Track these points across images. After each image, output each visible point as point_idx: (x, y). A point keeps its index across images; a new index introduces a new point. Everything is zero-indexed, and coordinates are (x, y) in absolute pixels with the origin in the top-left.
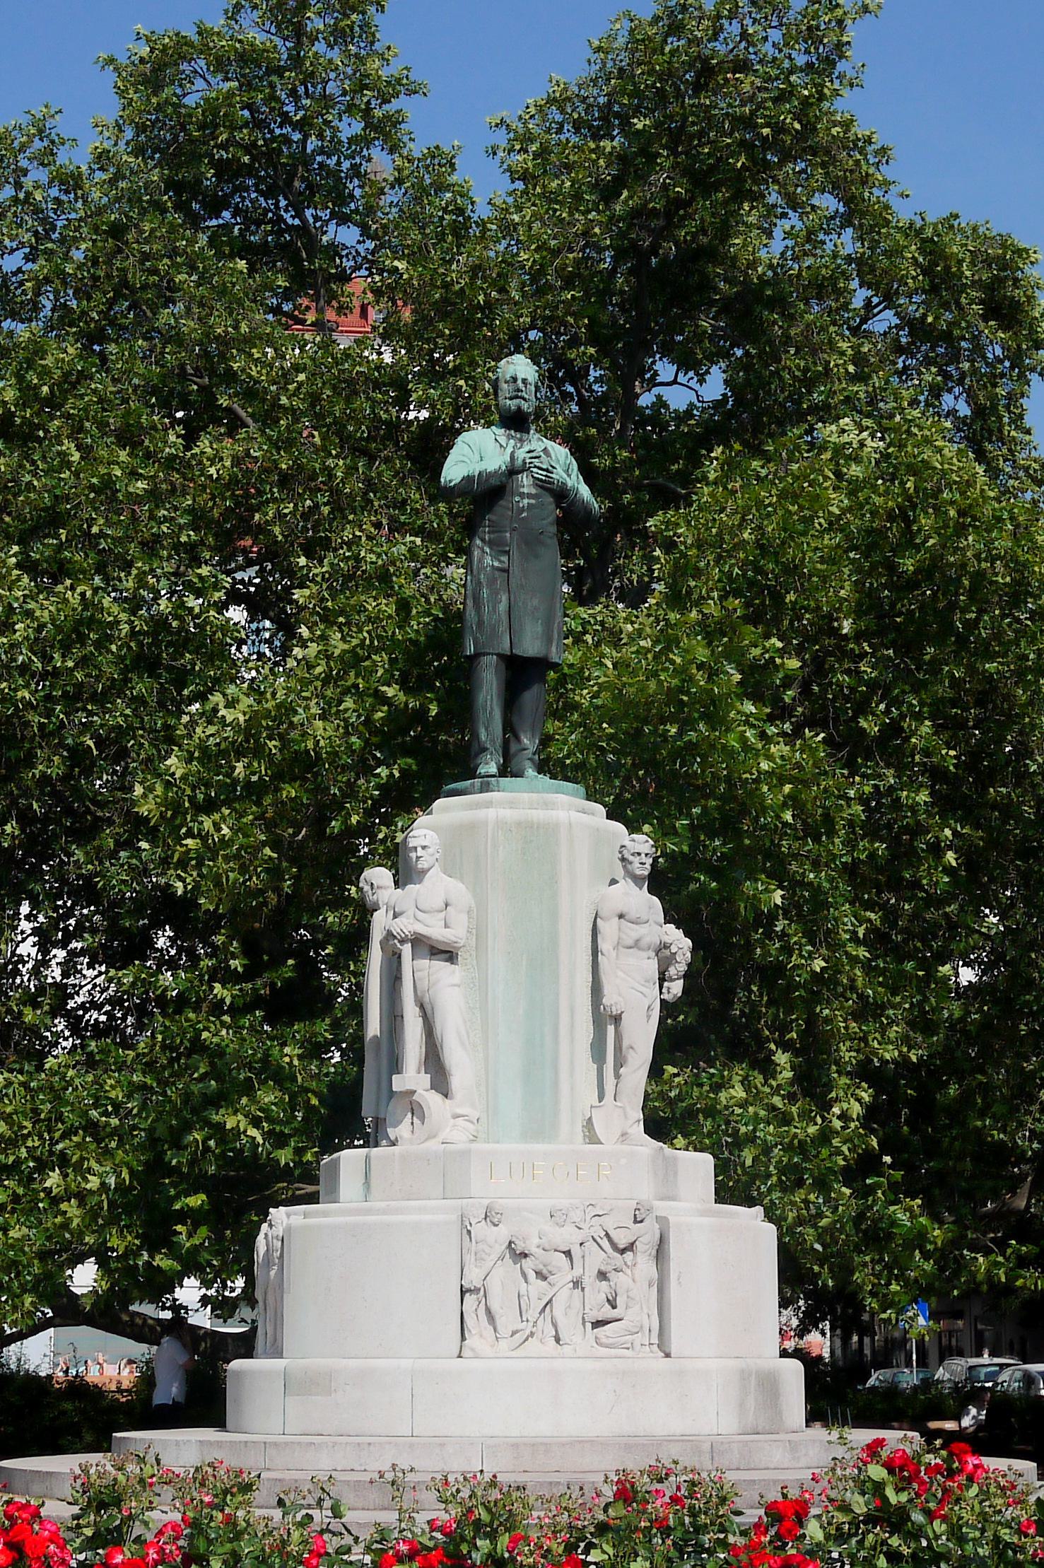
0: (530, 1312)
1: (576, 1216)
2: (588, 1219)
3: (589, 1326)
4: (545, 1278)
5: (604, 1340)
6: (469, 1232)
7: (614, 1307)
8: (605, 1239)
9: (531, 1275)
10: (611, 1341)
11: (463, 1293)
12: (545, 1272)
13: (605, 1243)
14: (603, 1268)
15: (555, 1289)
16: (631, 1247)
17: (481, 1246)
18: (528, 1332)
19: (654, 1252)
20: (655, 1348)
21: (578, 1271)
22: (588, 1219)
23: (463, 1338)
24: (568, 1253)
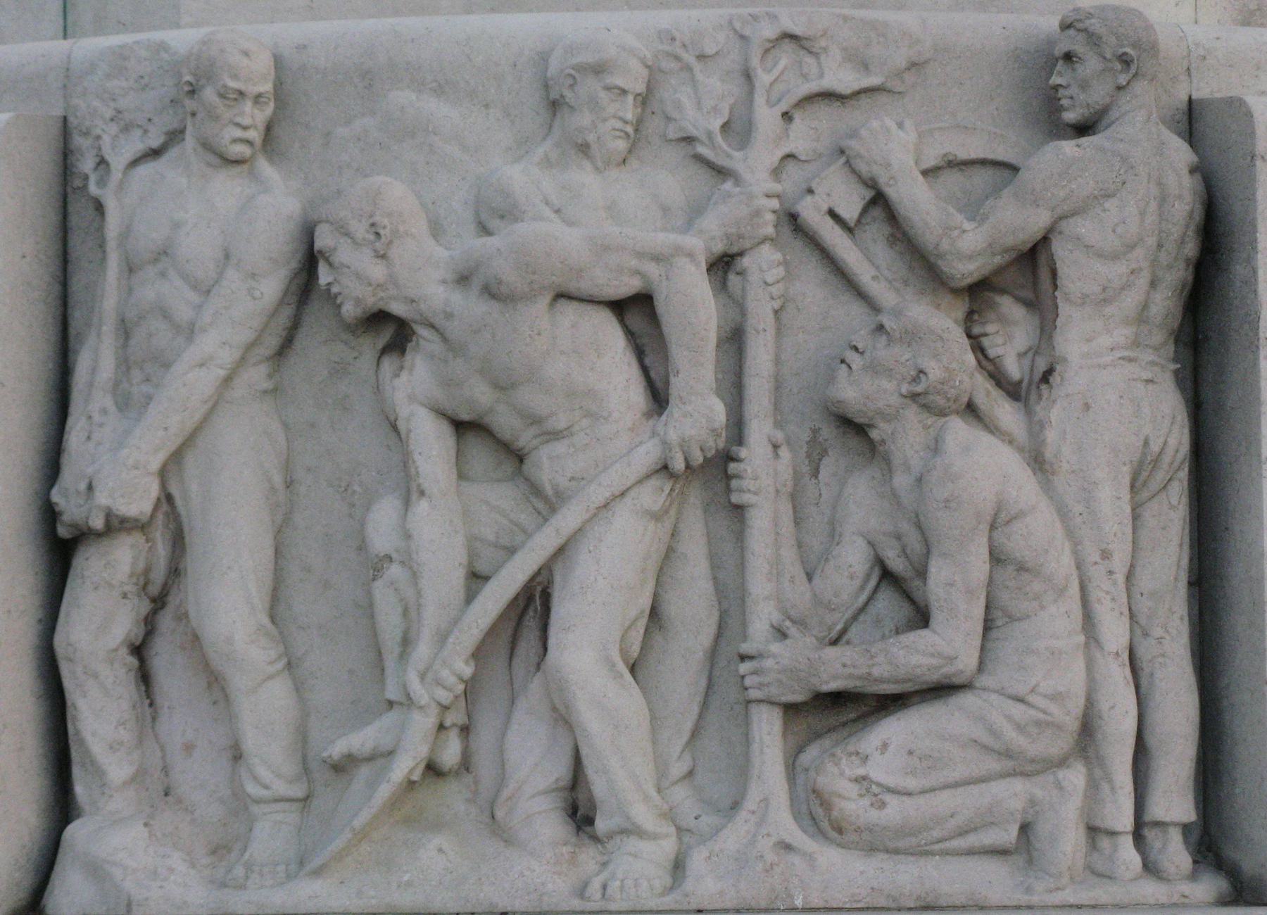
0: (423, 650)
1: (700, 106)
2: (766, 117)
3: (768, 729)
4: (515, 456)
5: (853, 806)
6: (99, 207)
7: (921, 617)
8: (876, 232)
9: (431, 445)
10: (895, 811)
11: (60, 549)
12: (505, 422)
13: (867, 259)
14: (851, 392)
15: (568, 519)
16: (1030, 269)
17: (149, 290)
18: (405, 765)
19: (1165, 303)
20: (1176, 854)
21: (698, 413)
23: (62, 806)
24: (636, 311)
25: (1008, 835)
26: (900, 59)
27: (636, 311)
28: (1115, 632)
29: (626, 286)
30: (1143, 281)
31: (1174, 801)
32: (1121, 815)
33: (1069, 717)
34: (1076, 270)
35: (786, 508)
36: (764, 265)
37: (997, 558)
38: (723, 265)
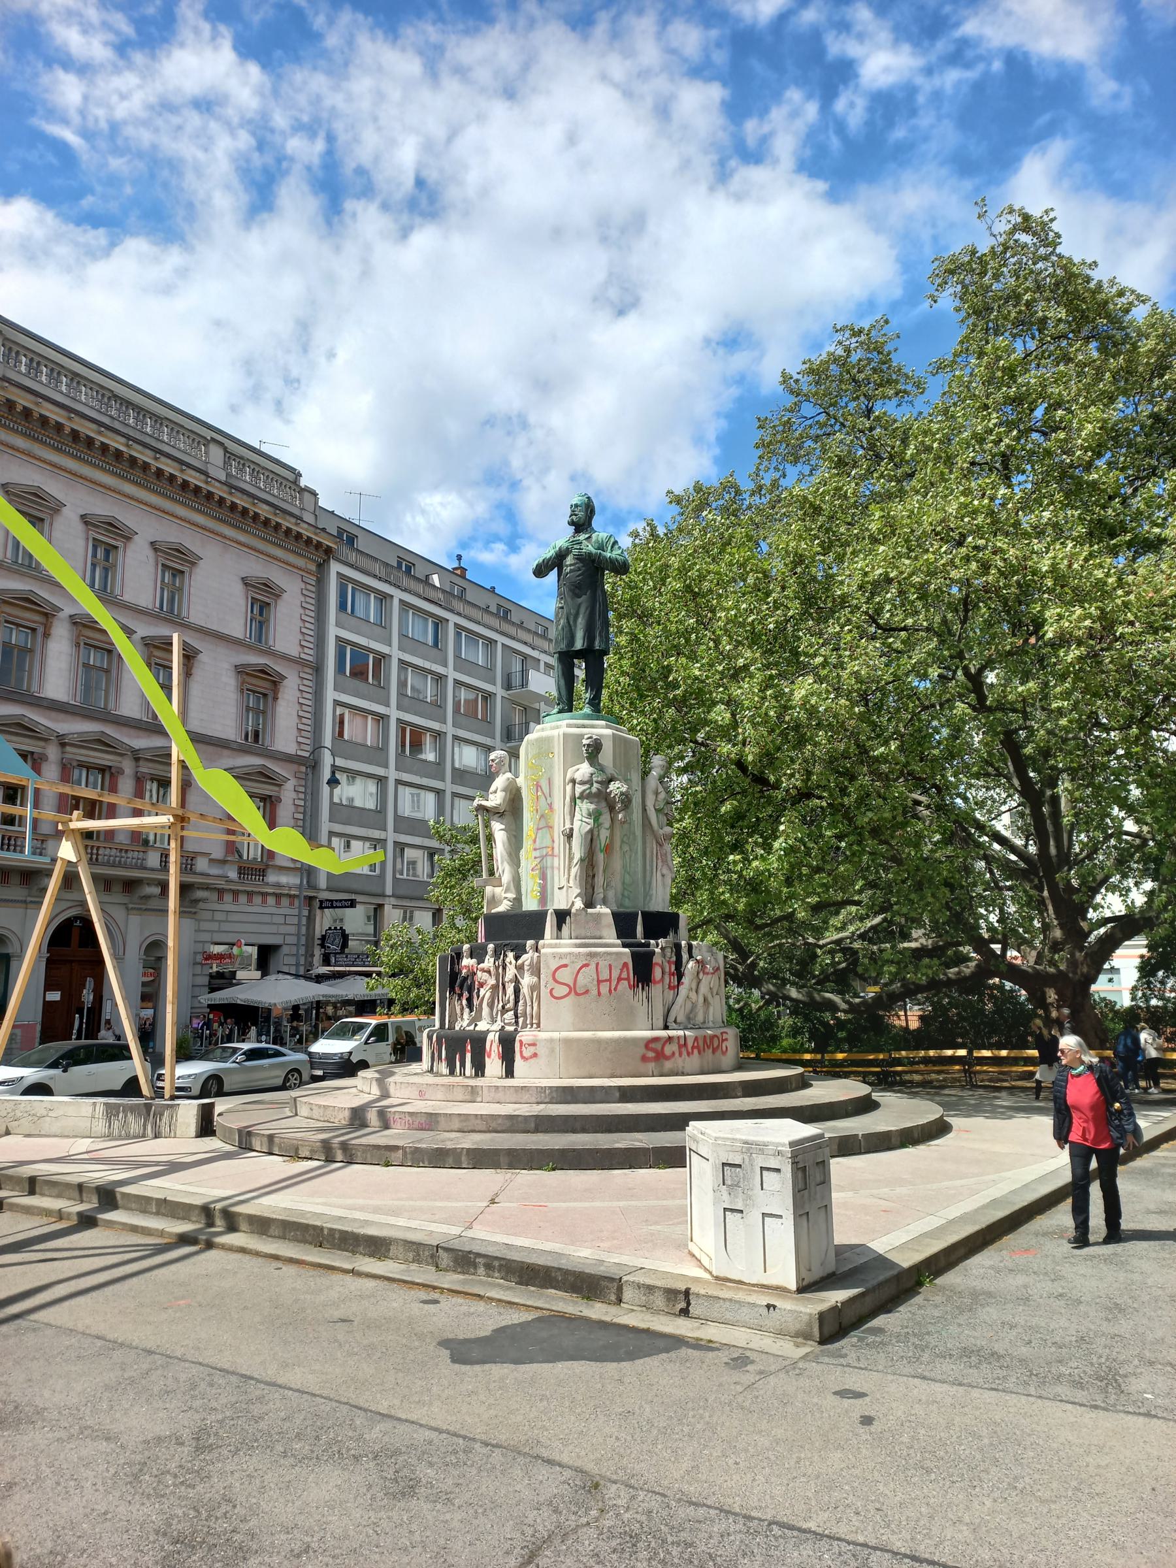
28: (529, 1003)
34: (526, 968)
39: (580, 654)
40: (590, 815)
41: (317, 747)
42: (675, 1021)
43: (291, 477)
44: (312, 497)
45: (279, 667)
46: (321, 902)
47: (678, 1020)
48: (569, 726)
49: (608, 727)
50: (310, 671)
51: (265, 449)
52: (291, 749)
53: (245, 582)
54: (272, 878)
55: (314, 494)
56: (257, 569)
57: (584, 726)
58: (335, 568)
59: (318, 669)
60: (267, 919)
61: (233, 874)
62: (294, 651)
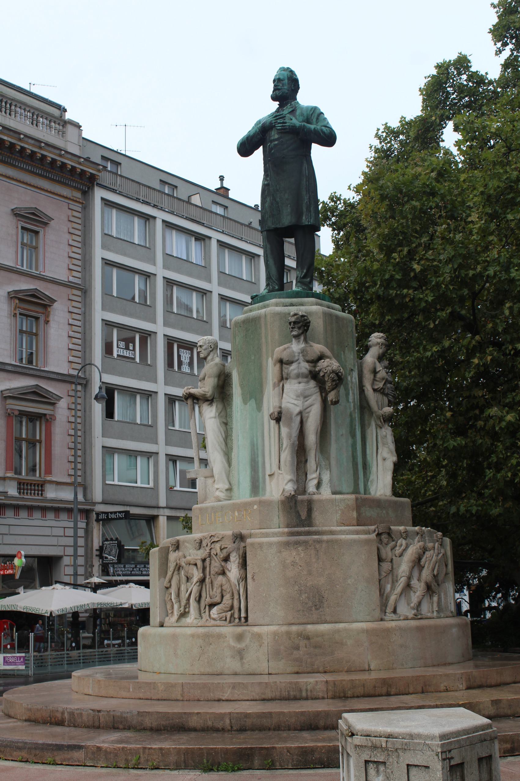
22: (209, 544)
24: (196, 565)
25: (224, 619)
26: (221, 537)
27: (196, 565)
28: (236, 597)
29: (194, 563)
30: (238, 559)
31: (243, 615)
32: (236, 615)
33: (229, 606)
35: (210, 585)
36: (208, 560)
37: (222, 590)
38: (204, 560)
39: (289, 231)
40: (298, 396)
41: (86, 364)
42: (395, 611)
43: (56, 112)
44: (76, 130)
45: (48, 290)
46: (98, 514)
47: (399, 610)
48: (277, 305)
49: (317, 304)
50: (78, 293)
51: (34, 90)
52: (63, 369)
53: (16, 214)
54: (51, 493)
55: (78, 126)
56: (25, 198)
57: (292, 305)
58: (99, 194)
59: (85, 291)
60: (47, 531)
61: (13, 491)
62: (62, 275)
